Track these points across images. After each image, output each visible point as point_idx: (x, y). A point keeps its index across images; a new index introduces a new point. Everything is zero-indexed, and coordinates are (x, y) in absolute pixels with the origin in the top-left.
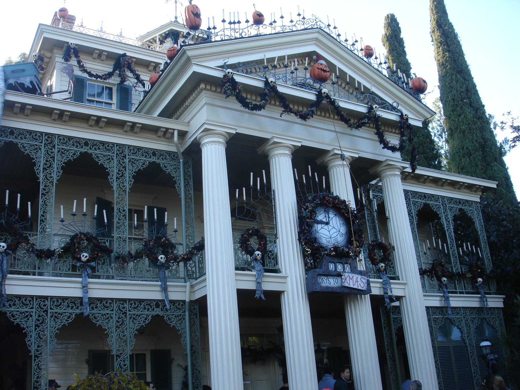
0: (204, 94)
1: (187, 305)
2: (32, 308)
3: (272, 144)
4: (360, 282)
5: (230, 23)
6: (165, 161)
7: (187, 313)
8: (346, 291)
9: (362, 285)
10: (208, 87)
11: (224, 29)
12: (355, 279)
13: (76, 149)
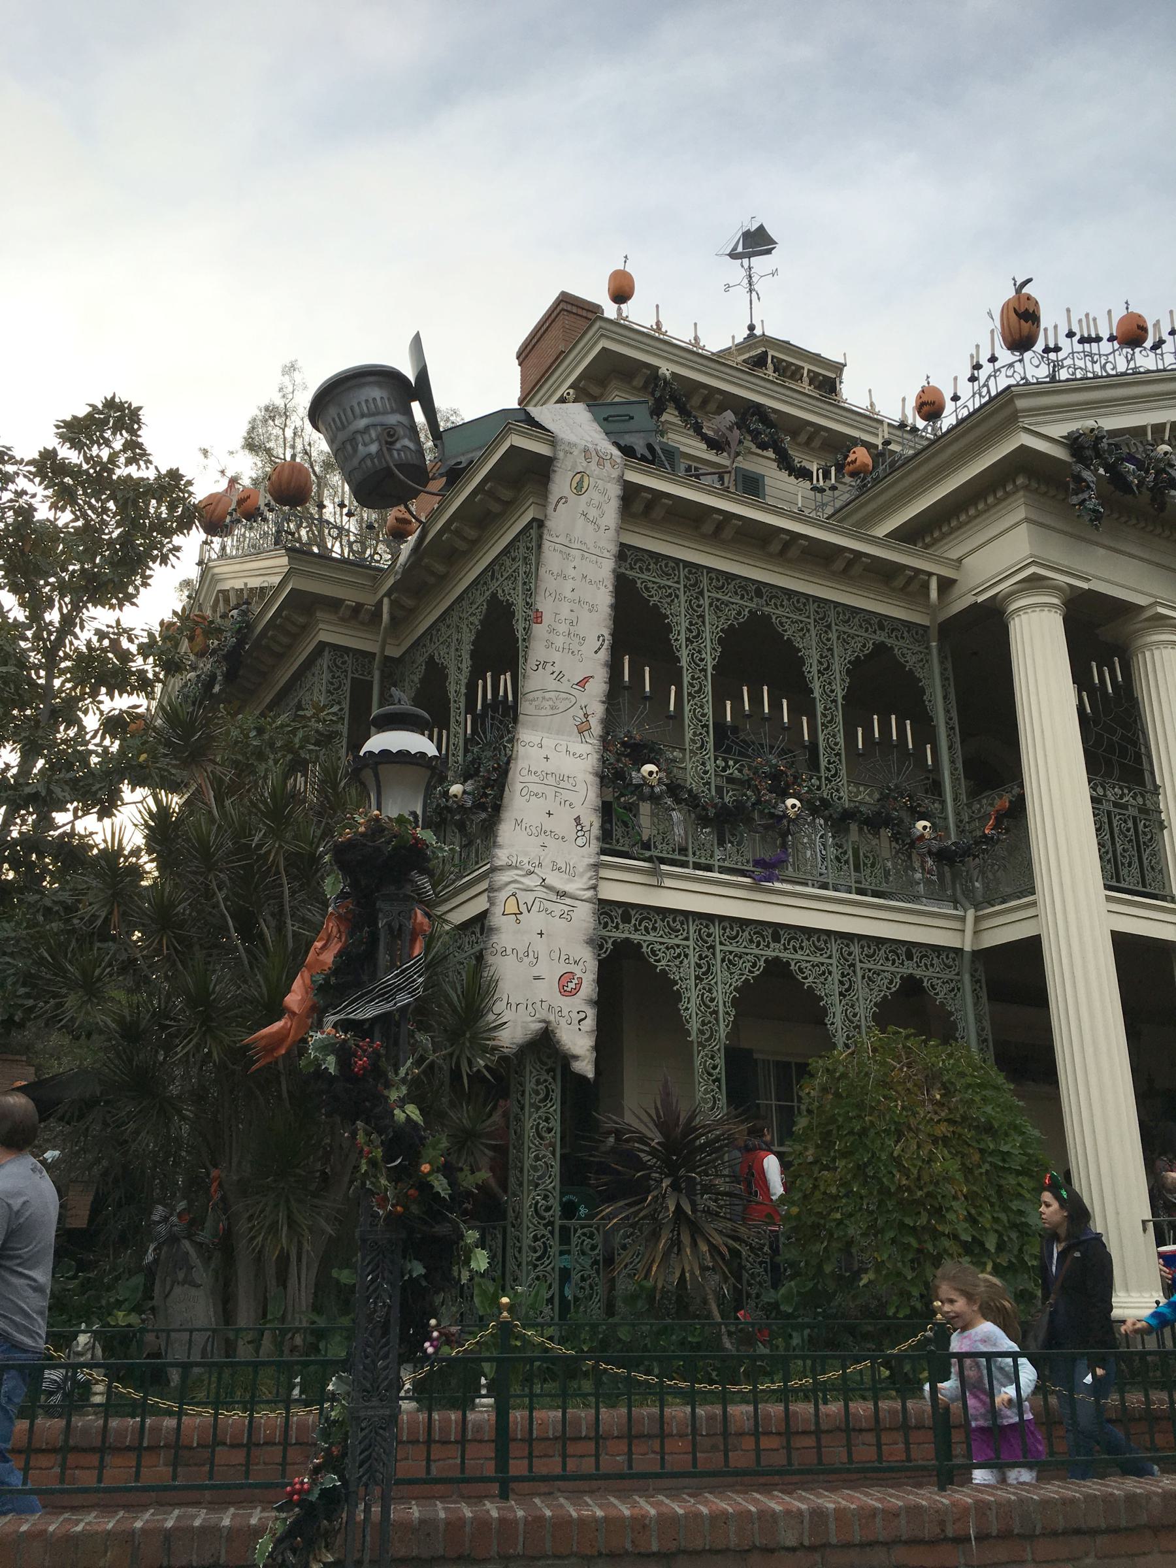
0: (1020, 498)
1: (967, 960)
2: (687, 939)
3: (1147, 620)
5: (1082, 341)
6: (901, 643)
7: (967, 978)
10: (1034, 485)
11: (1073, 353)
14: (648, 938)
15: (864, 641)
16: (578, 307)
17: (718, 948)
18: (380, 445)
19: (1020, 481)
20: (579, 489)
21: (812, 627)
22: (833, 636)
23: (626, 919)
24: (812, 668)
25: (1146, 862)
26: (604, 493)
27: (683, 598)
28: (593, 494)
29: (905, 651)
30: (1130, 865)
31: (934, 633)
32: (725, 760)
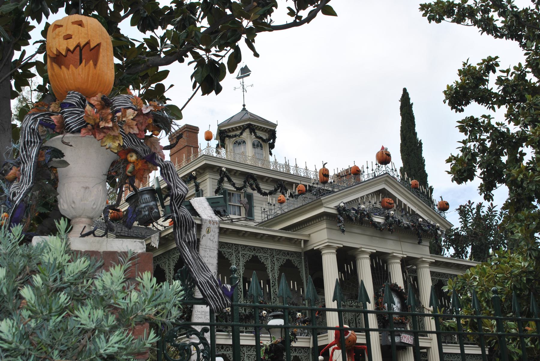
1: (311, 350)
4: (410, 340)
8: (403, 345)
9: (411, 341)
12: (407, 337)
13: (250, 253)
14: (228, 353)
15: (283, 259)
16: (191, 129)
17: (246, 353)
18: (149, 212)
19: (324, 218)
20: (208, 232)
21: (269, 258)
22: (275, 259)
23: (222, 348)
24: (269, 270)
25: (357, 321)
26: (214, 232)
27: (234, 254)
28: (212, 233)
29: (295, 261)
30: (353, 323)
31: (303, 254)
32: (246, 301)
